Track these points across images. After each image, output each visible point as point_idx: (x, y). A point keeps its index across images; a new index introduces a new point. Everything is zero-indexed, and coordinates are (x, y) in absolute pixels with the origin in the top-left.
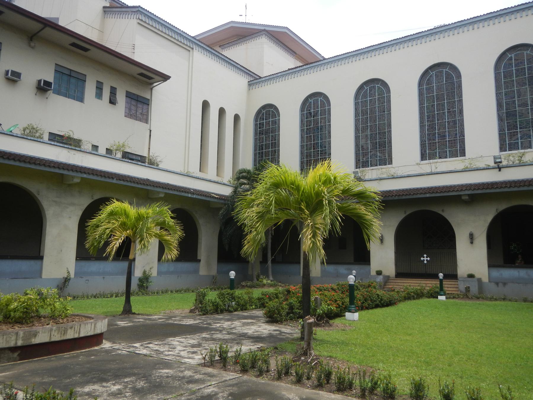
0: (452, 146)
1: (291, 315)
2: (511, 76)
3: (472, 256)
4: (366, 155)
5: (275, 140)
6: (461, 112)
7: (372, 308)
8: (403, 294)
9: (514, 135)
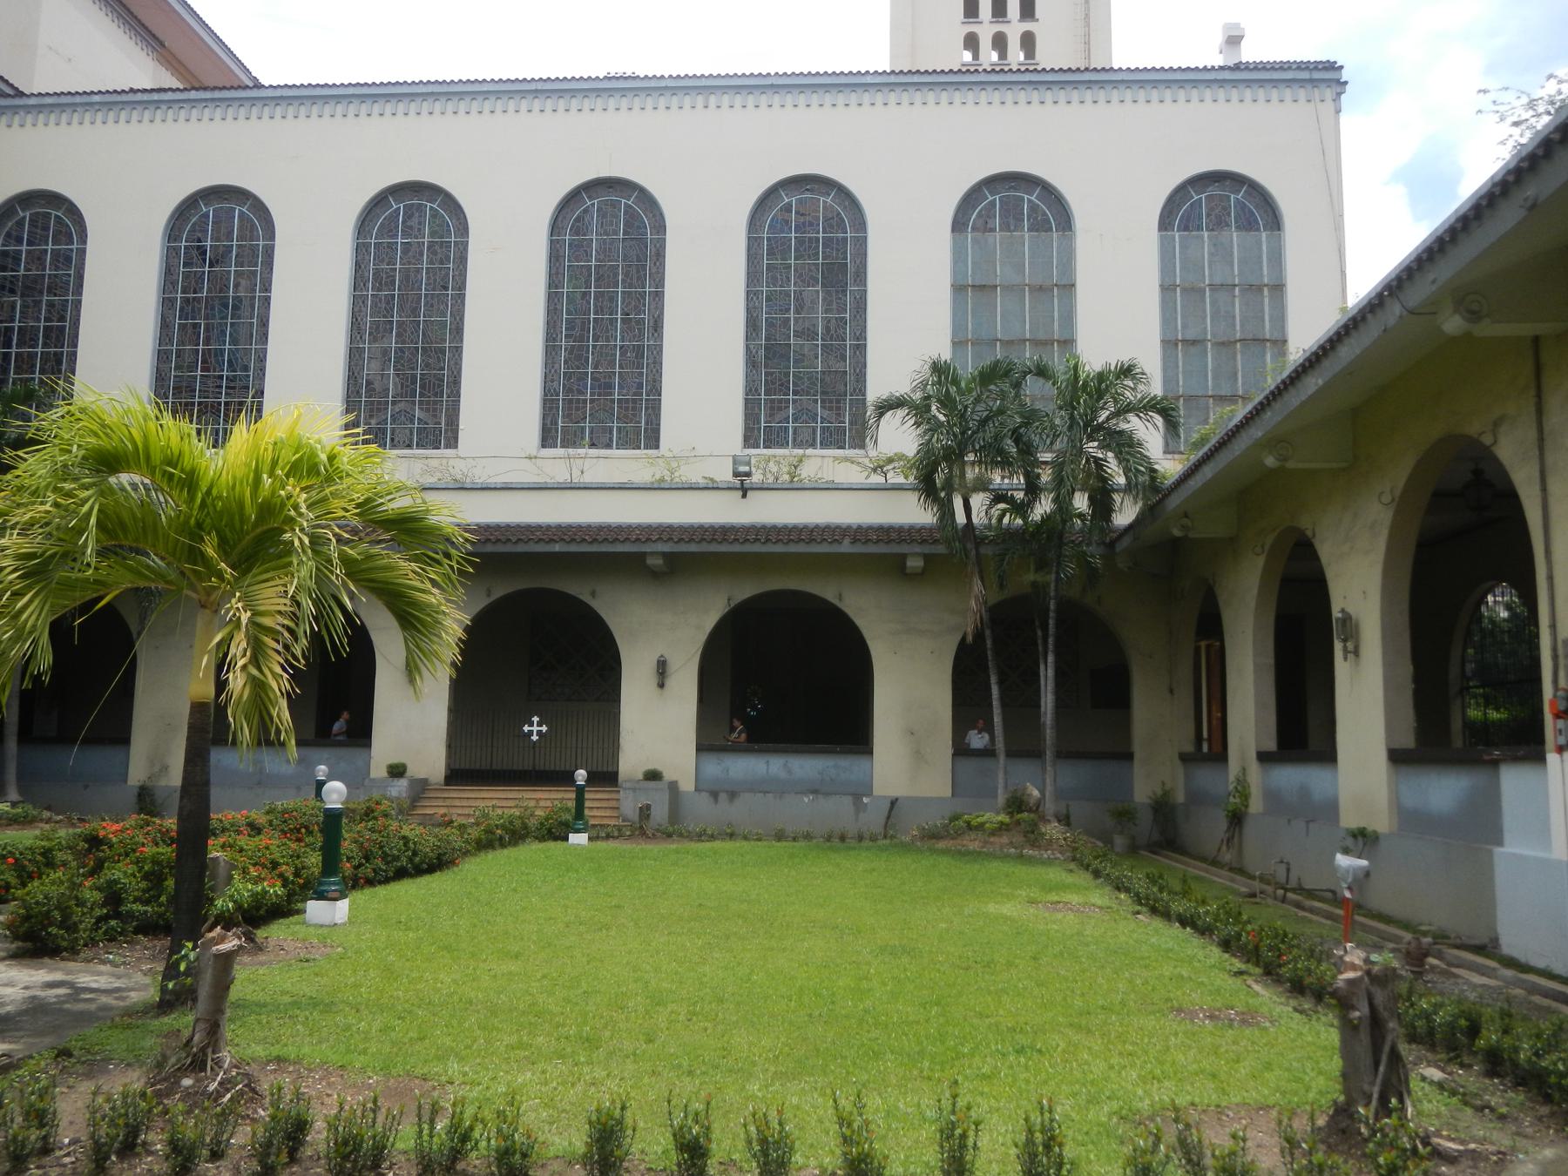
0: (626, 416)
1: (113, 923)
2: (785, 254)
3: (658, 723)
4: (379, 410)
5: (62, 319)
6: (657, 326)
7: (387, 881)
8: (475, 833)
9: (780, 409)
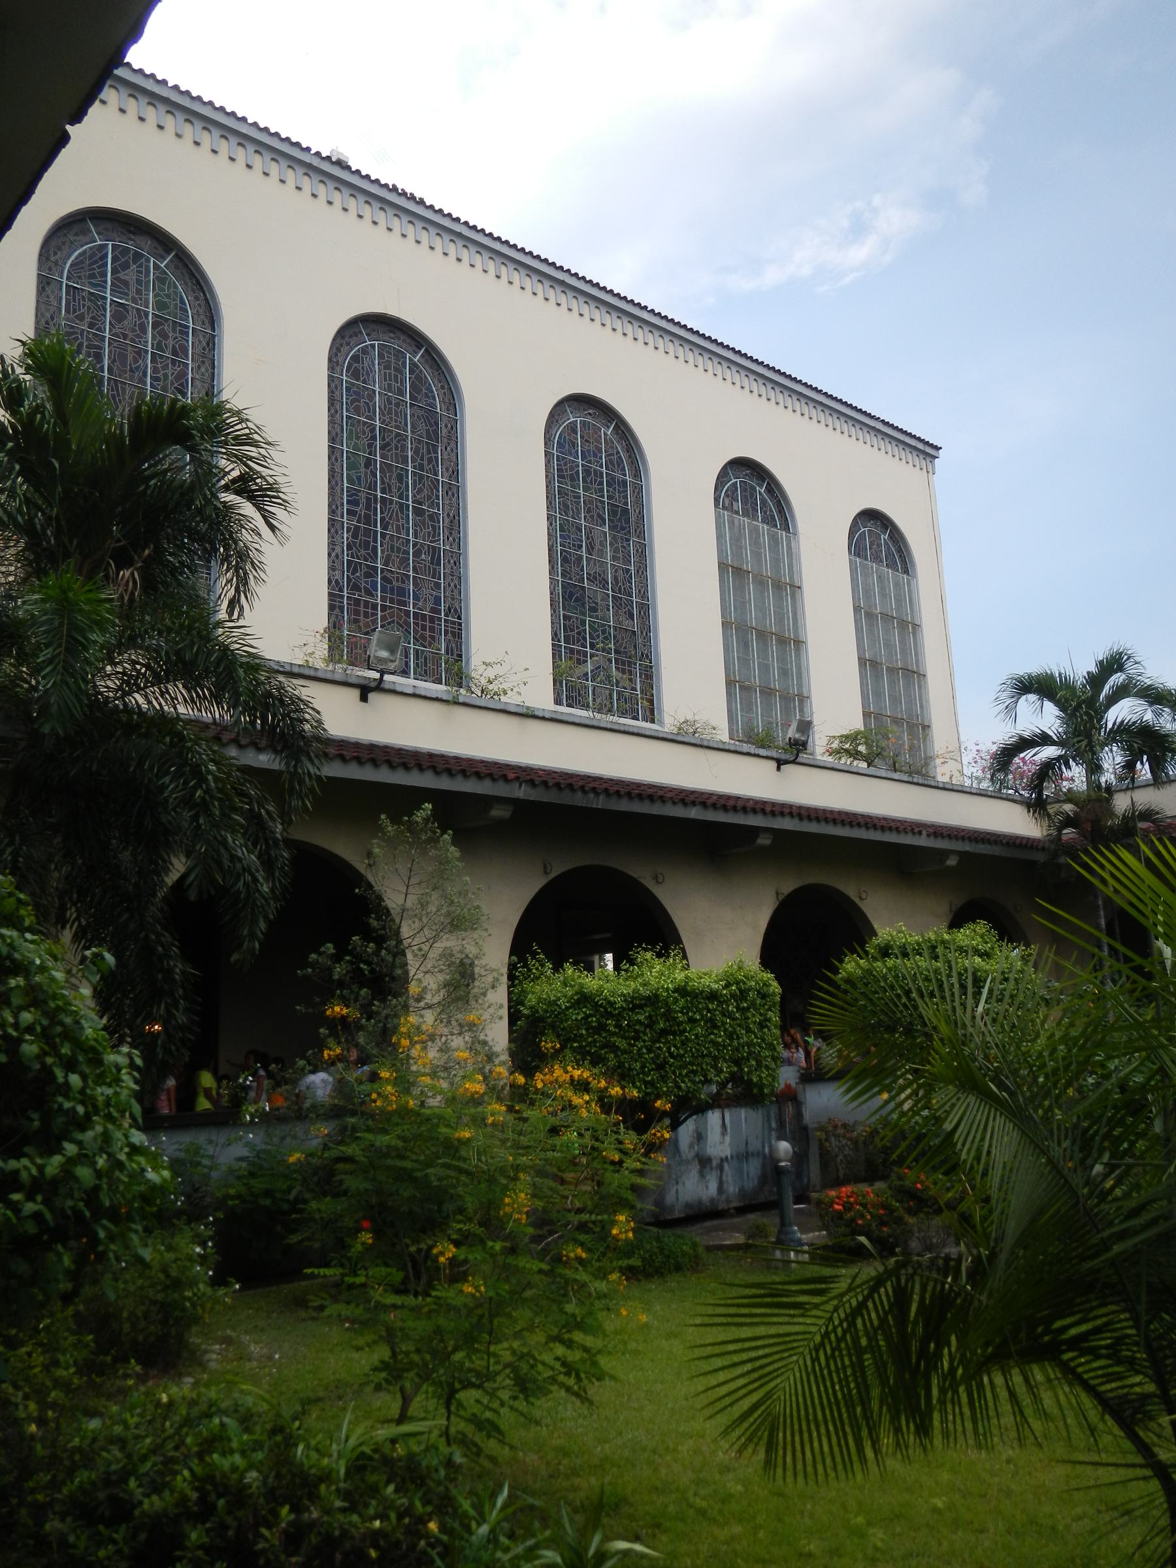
0: (423, 637)
